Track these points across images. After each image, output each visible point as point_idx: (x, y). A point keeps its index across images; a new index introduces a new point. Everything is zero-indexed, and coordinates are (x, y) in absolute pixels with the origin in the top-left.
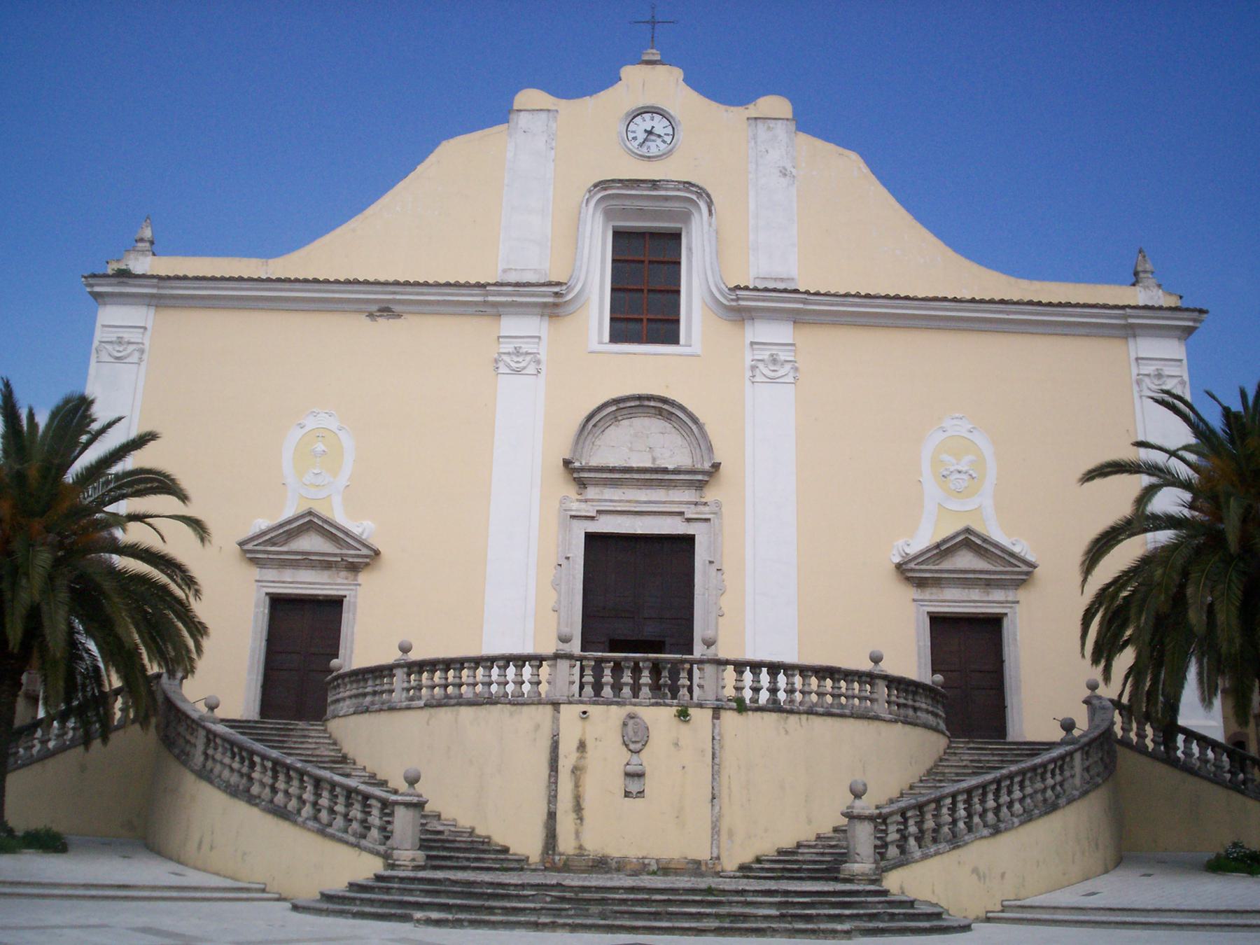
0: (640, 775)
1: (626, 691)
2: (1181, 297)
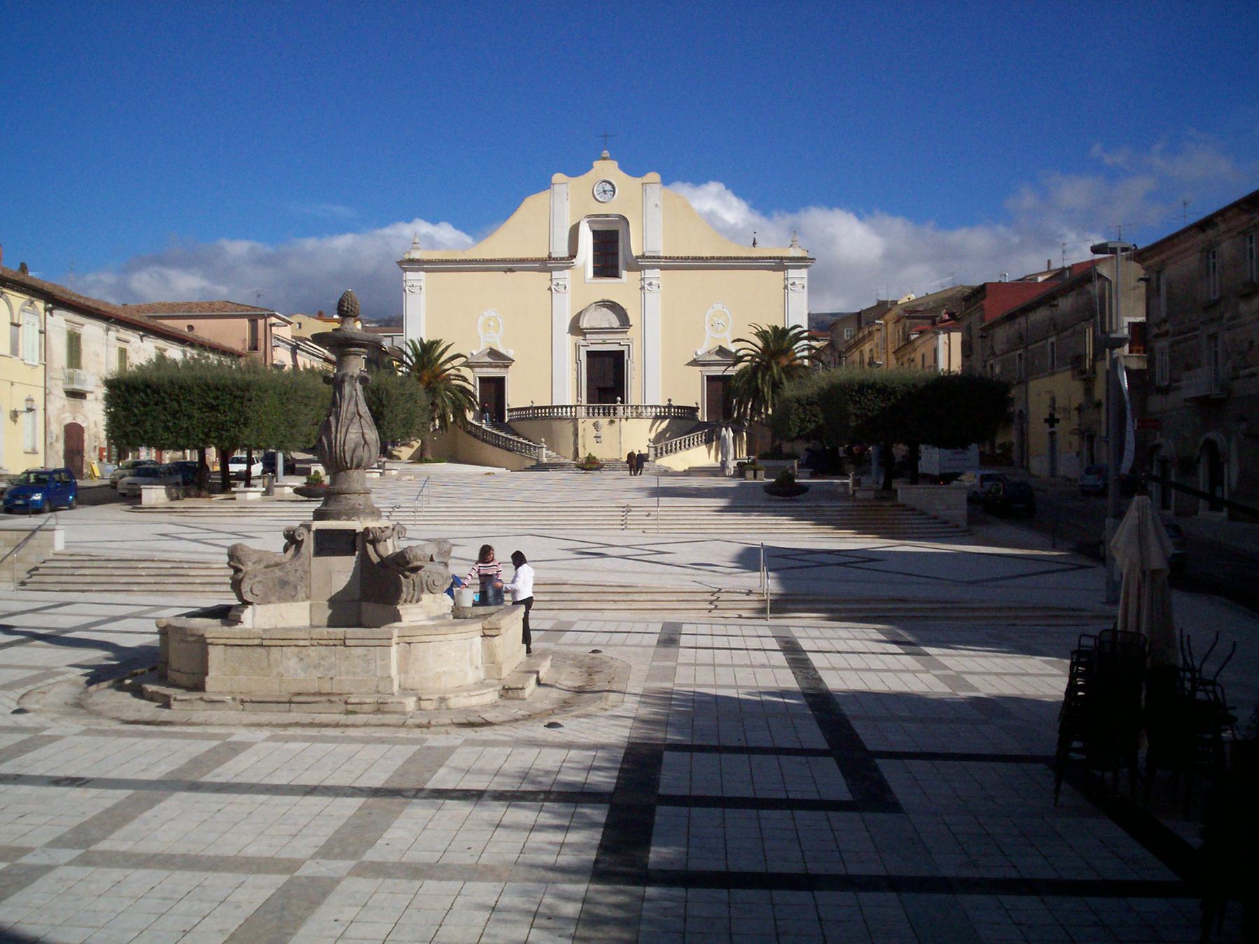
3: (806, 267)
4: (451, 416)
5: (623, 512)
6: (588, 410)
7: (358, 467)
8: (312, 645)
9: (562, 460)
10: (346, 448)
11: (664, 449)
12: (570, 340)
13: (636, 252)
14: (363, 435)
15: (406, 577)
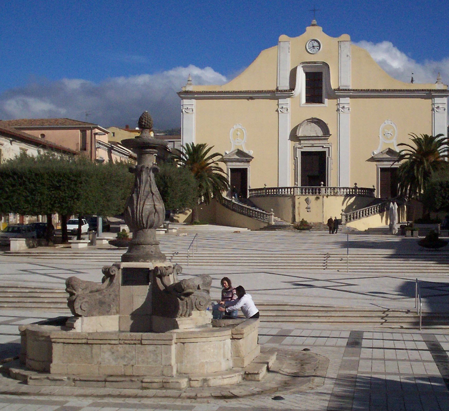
0: (309, 208)
1: (307, 193)
2: (448, 86)
3: (446, 96)
4: (212, 194)
5: (325, 257)
6: (302, 190)
7: (151, 227)
8: (120, 344)
9: (285, 223)
10: (143, 214)
11: (352, 216)
12: (290, 144)
13: (334, 86)
14: (154, 206)
15: (182, 299)
